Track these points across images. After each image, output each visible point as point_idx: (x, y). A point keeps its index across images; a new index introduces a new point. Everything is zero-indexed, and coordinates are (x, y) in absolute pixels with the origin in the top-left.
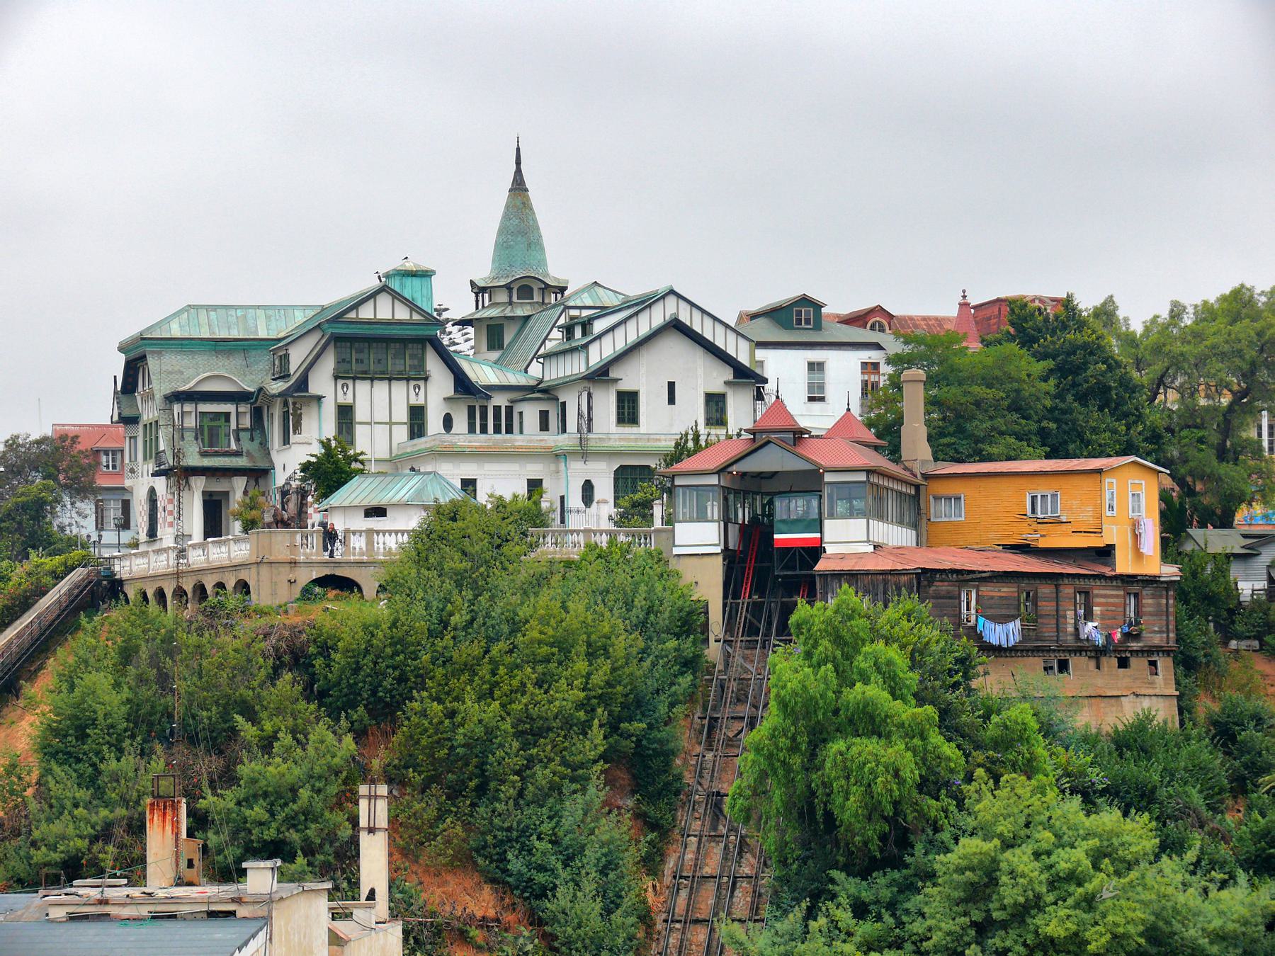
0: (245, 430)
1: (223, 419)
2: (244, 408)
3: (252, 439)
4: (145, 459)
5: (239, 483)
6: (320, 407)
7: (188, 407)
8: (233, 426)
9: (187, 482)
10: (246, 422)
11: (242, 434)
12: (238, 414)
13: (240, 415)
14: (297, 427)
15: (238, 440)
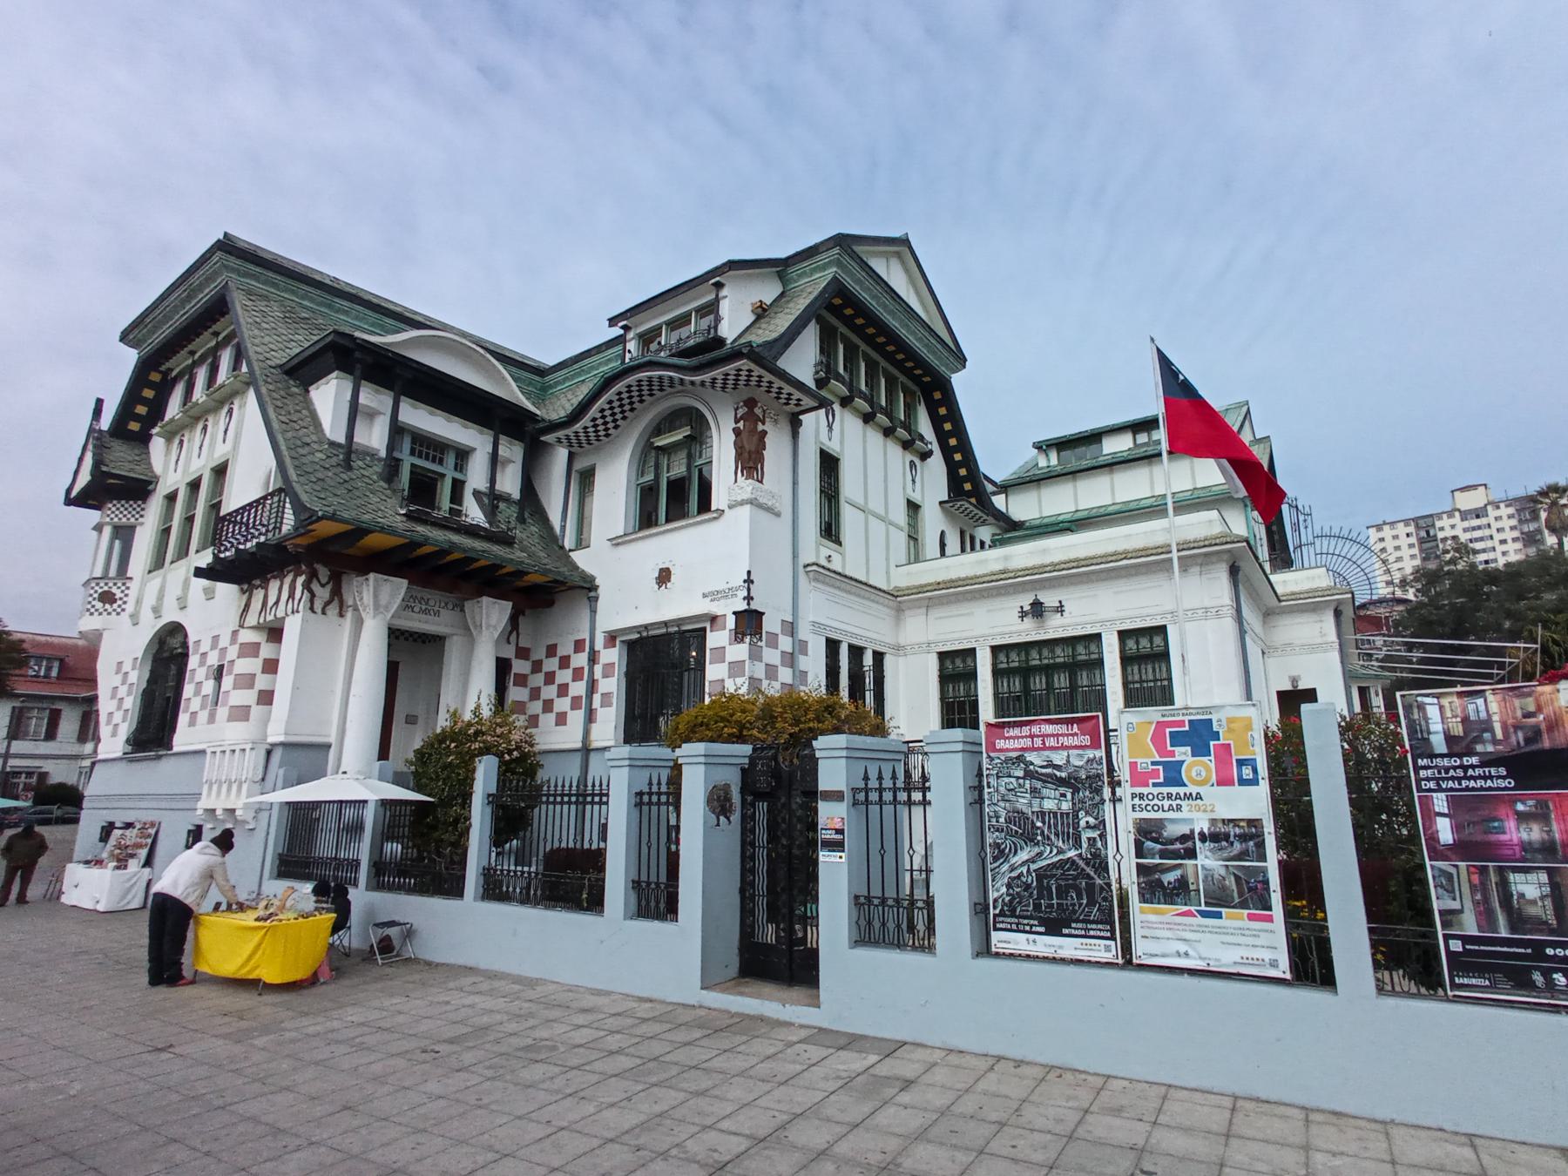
0: (506, 498)
1: (450, 460)
2: (512, 451)
3: (521, 520)
4: (158, 563)
5: (493, 614)
6: (795, 435)
7: (370, 397)
8: (476, 476)
9: (337, 593)
10: (510, 483)
11: (502, 505)
12: (495, 461)
13: (484, 466)
14: (750, 460)
15: (491, 511)
